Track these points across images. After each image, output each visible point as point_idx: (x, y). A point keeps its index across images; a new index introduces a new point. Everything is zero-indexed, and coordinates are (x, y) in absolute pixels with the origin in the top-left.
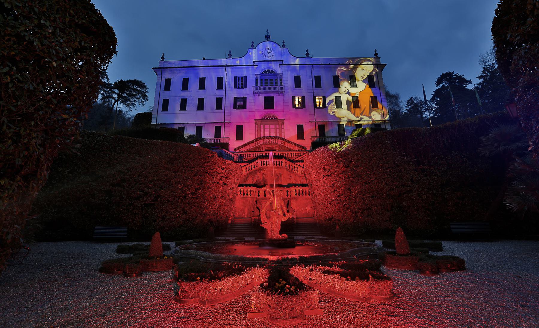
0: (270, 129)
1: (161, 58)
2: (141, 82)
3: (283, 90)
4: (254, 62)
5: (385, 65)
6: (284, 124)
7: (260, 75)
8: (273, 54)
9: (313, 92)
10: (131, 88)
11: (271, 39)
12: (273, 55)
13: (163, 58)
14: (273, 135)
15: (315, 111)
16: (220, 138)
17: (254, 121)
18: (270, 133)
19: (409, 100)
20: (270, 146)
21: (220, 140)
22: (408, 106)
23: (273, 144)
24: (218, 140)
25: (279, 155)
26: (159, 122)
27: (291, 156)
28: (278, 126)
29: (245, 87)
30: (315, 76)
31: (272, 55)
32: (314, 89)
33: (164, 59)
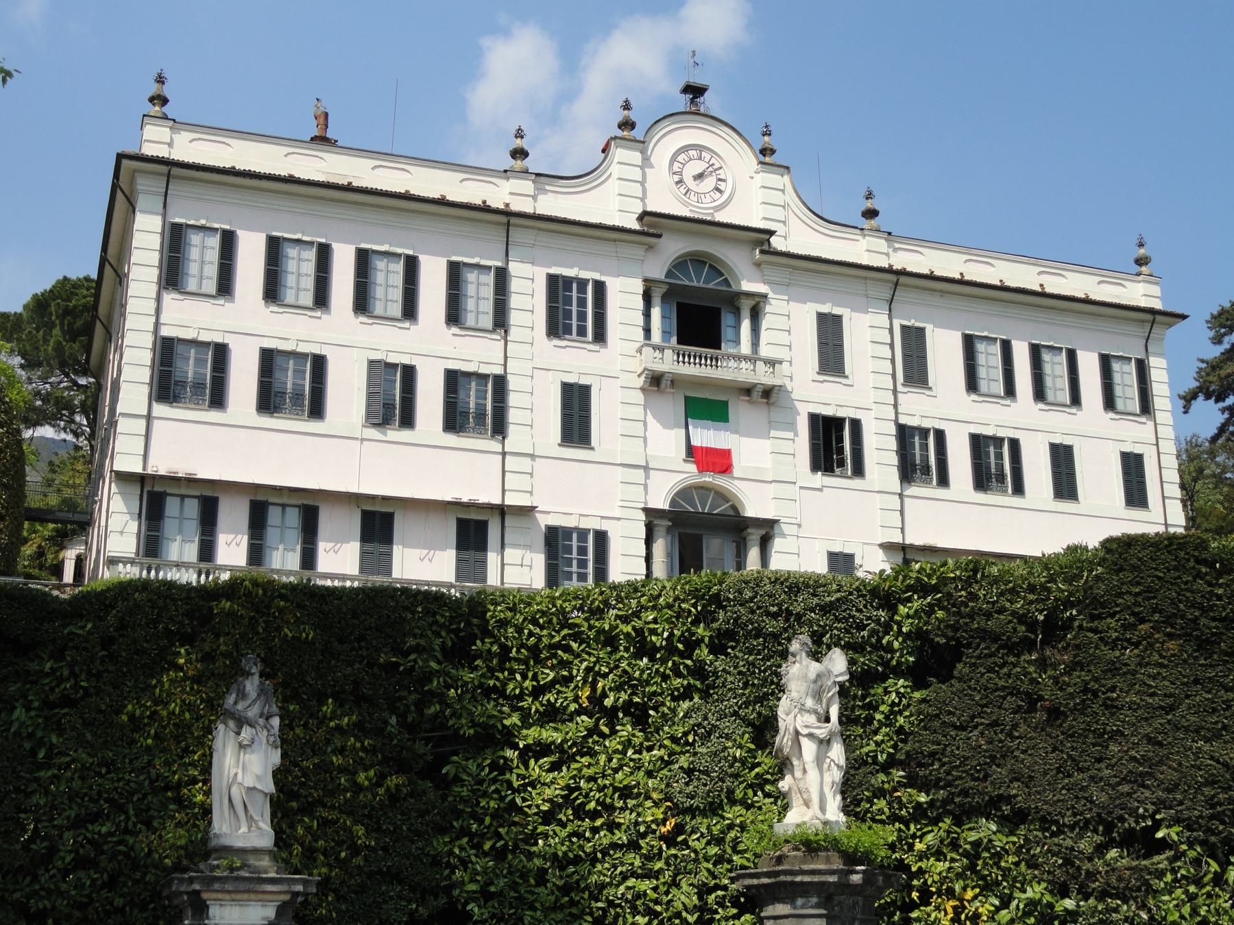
1: (152, 100)
3: (777, 382)
5: (1184, 317)
8: (722, 186)
9: (895, 406)
11: (709, 102)
12: (720, 191)
13: (160, 100)
15: (901, 495)
26: (160, 465)
29: (600, 336)
30: (903, 327)
31: (718, 189)
32: (900, 388)
33: (164, 101)
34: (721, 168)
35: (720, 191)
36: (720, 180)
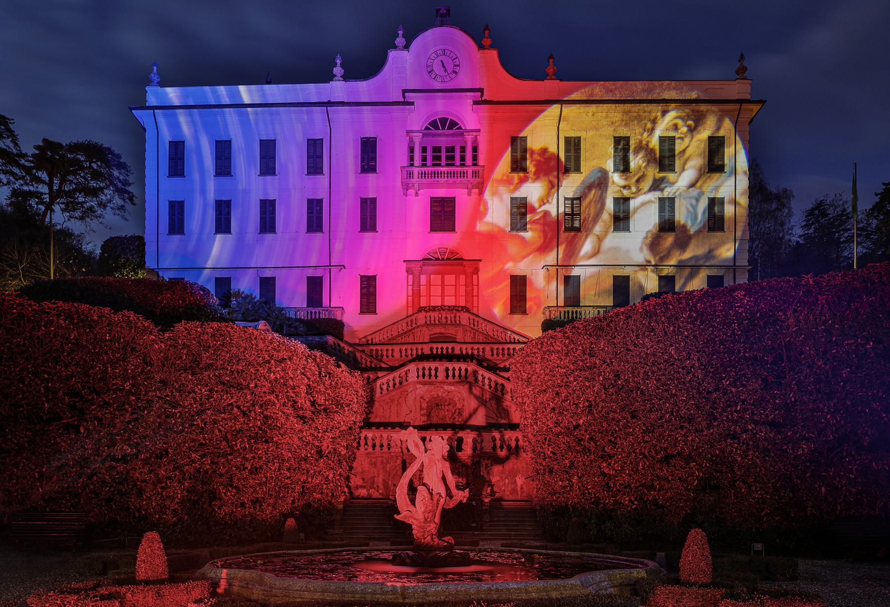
0: (443, 285)
2: (109, 149)
4: (405, 91)
6: (477, 274)
7: (421, 134)
10: (82, 168)
12: (456, 73)
14: (450, 301)
16: (319, 309)
17: (405, 264)
18: (443, 296)
19: (812, 210)
20: (443, 331)
21: (319, 313)
22: (807, 226)
23: (449, 324)
24: (316, 313)
25: (462, 353)
27: (493, 355)
28: (462, 278)
34: (457, 58)
35: (456, 73)
36: (456, 66)
